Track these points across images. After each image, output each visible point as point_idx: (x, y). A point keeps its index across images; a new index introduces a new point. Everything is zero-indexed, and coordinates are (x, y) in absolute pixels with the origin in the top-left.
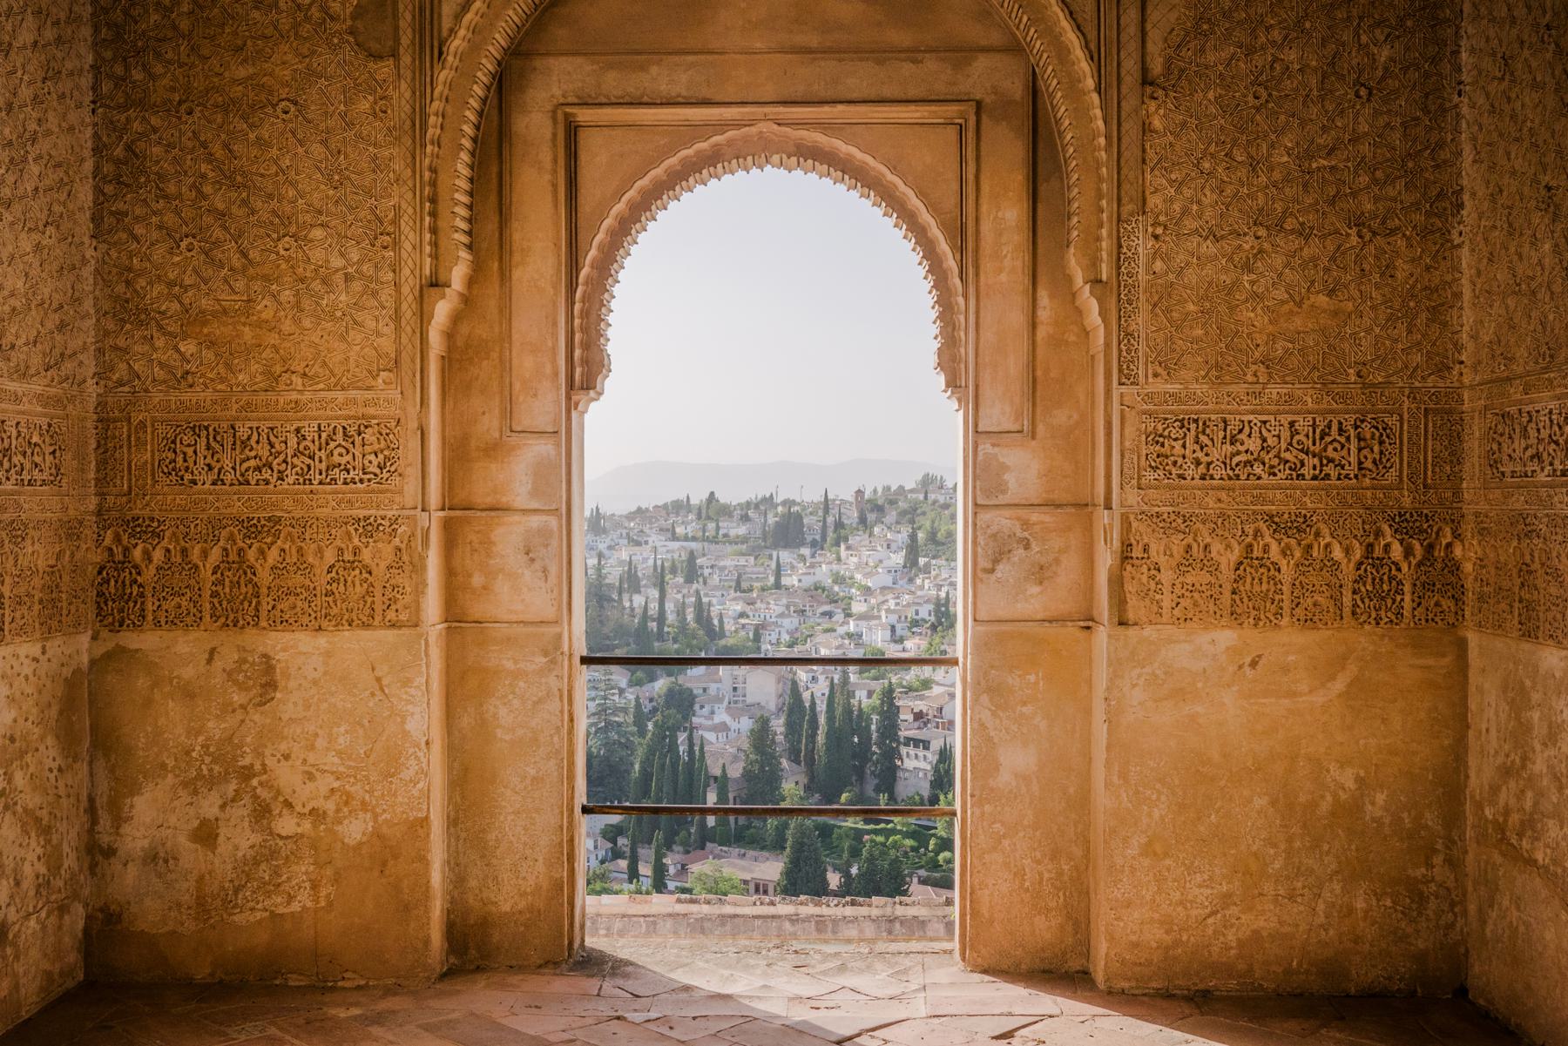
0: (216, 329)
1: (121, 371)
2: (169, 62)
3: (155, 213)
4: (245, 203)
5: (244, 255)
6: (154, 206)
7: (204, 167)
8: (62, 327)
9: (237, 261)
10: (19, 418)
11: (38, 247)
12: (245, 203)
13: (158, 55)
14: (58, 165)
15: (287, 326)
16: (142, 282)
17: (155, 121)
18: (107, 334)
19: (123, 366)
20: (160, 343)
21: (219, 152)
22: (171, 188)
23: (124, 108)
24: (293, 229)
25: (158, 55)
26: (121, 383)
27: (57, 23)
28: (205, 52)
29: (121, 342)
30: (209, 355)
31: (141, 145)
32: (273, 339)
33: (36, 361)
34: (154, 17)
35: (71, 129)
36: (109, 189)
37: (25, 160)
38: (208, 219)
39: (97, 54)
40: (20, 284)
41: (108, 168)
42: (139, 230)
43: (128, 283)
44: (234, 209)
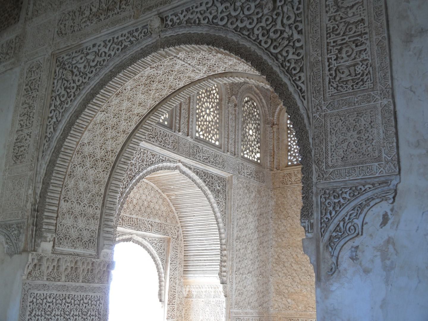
0: (295, 297)
1: (276, 306)
2: (285, 237)
3: (283, 270)
4: (300, 268)
5: (300, 279)
6: (283, 269)
7: (292, 260)
8: (263, 296)
9: (299, 281)
10: (253, 318)
11: (258, 280)
12: (300, 268)
13: (283, 236)
14: (263, 261)
15: (309, 296)
16: (280, 286)
17: (283, 250)
18: (274, 297)
19: (277, 304)
20: (284, 299)
21: (295, 257)
22: (286, 265)
23: (277, 247)
24: (310, 274)
25: (283, 236)
26: (276, 308)
27: (263, 232)
28: (292, 235)
29: (276, 299)
30: (293, 302)
31: (280, 255)
32: (306, 299)
33: (257, 305)
34: (283, 228)
35: (266, 253)
36: (274, 265)
37: (255, 262)
38: (293, 271)
39: (273, 236)
40: (253, 289)
41: (274, 260)
42: (280, 274)
43: (278, 285)
44: (298, 269)
